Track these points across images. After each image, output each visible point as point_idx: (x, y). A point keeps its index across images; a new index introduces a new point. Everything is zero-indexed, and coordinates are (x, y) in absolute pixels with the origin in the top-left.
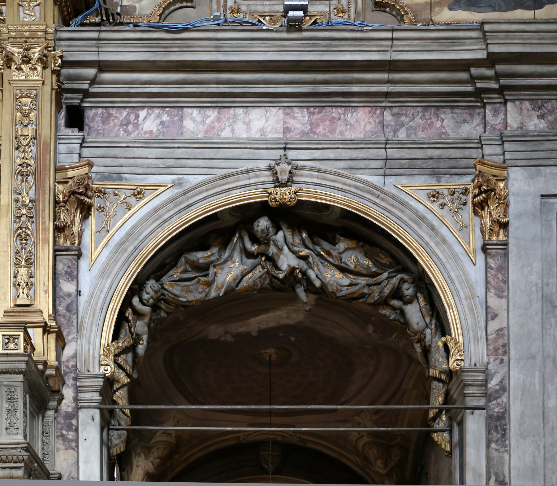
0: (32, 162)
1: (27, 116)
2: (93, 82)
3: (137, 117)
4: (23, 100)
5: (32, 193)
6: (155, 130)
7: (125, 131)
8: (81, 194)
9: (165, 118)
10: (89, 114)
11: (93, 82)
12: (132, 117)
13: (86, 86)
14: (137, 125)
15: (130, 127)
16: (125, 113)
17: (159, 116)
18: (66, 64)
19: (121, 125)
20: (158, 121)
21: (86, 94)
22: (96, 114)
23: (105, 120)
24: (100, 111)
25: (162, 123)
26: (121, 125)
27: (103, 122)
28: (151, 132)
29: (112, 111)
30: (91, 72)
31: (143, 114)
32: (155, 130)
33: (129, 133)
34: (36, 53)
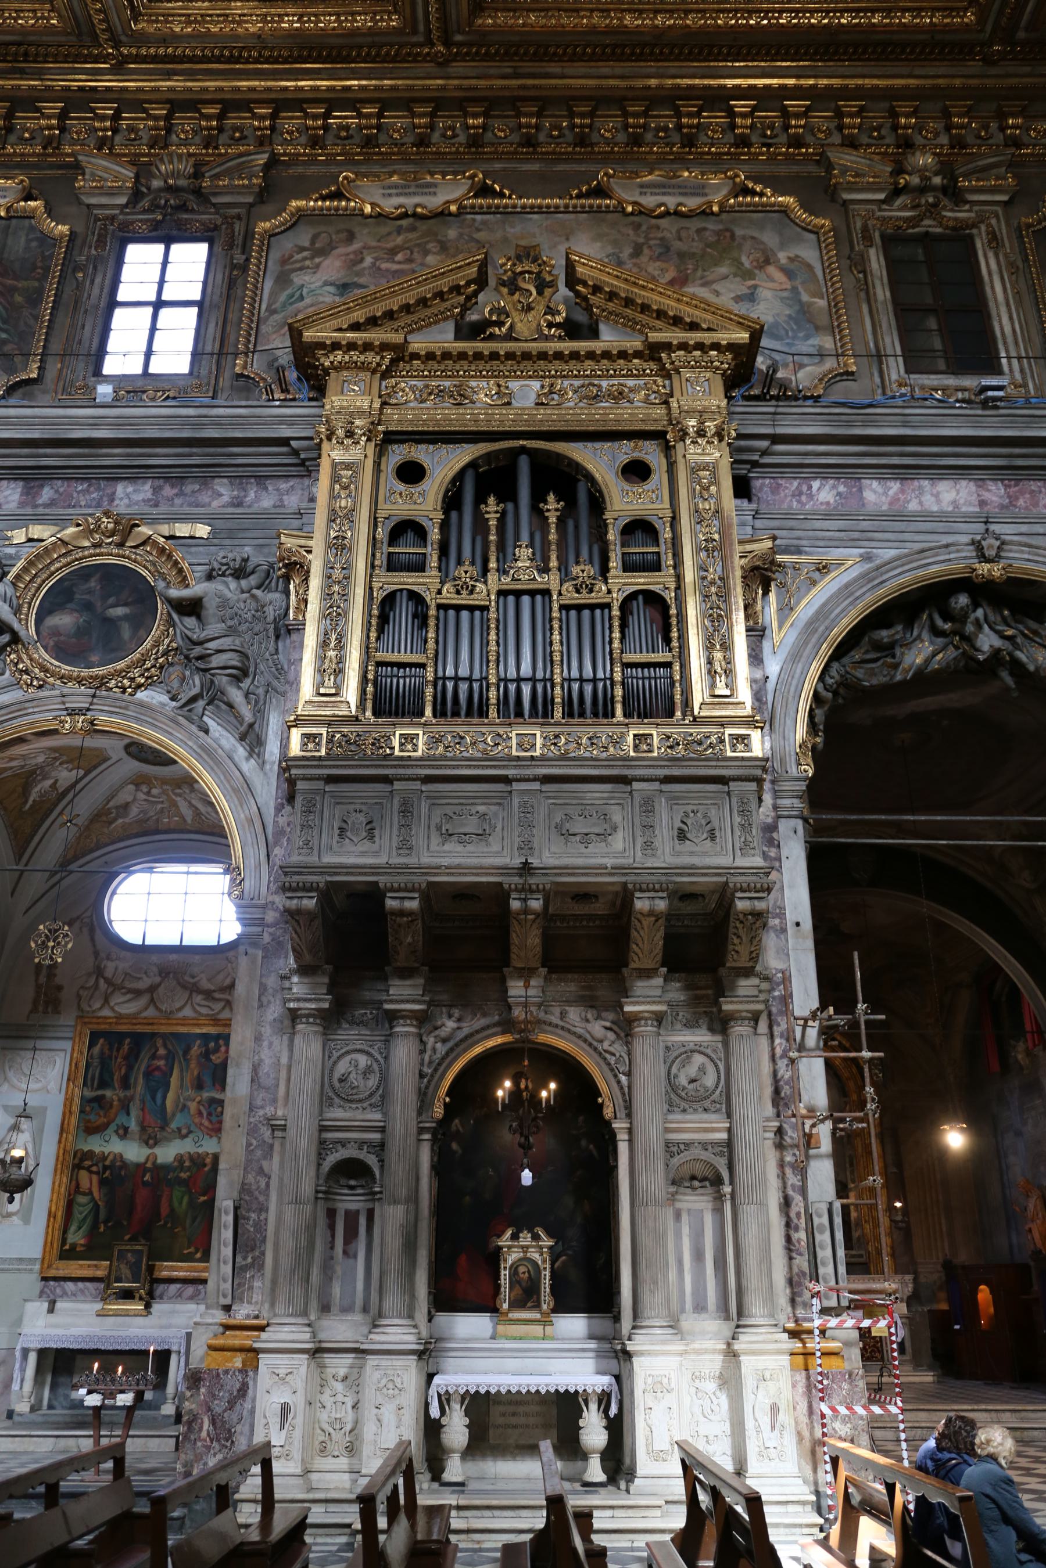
0: (716, 537)
1: (707, 489)
2: (764, 453)
3: (810, 487)
4: (701, 473)
5: (719, 569)
6: (832, 501)
7: (799, 502)
8: (766, 570)
9: (842, 488)
10: (756, 484)
11: (764, 453)
12: (805, 488)
13: (756, 458)
14: (811, 496)
15: (804, 498)
16: (796, 483)
17: (834, 487)
18: (740, 436)
19: (793, 496)
20: (834, 492)
21: (755, 464)
22: (763, 485)
23: (775, 490)
24: (767, 481)
25: (839, 494)
26: (793, 496)
27: (773, 493)
28: (828, 503)
29: (780, 481)
30: (764, 444)
31: (816, 484)
32: (832, 501)
33: (804, 505)
34: (711, 426)
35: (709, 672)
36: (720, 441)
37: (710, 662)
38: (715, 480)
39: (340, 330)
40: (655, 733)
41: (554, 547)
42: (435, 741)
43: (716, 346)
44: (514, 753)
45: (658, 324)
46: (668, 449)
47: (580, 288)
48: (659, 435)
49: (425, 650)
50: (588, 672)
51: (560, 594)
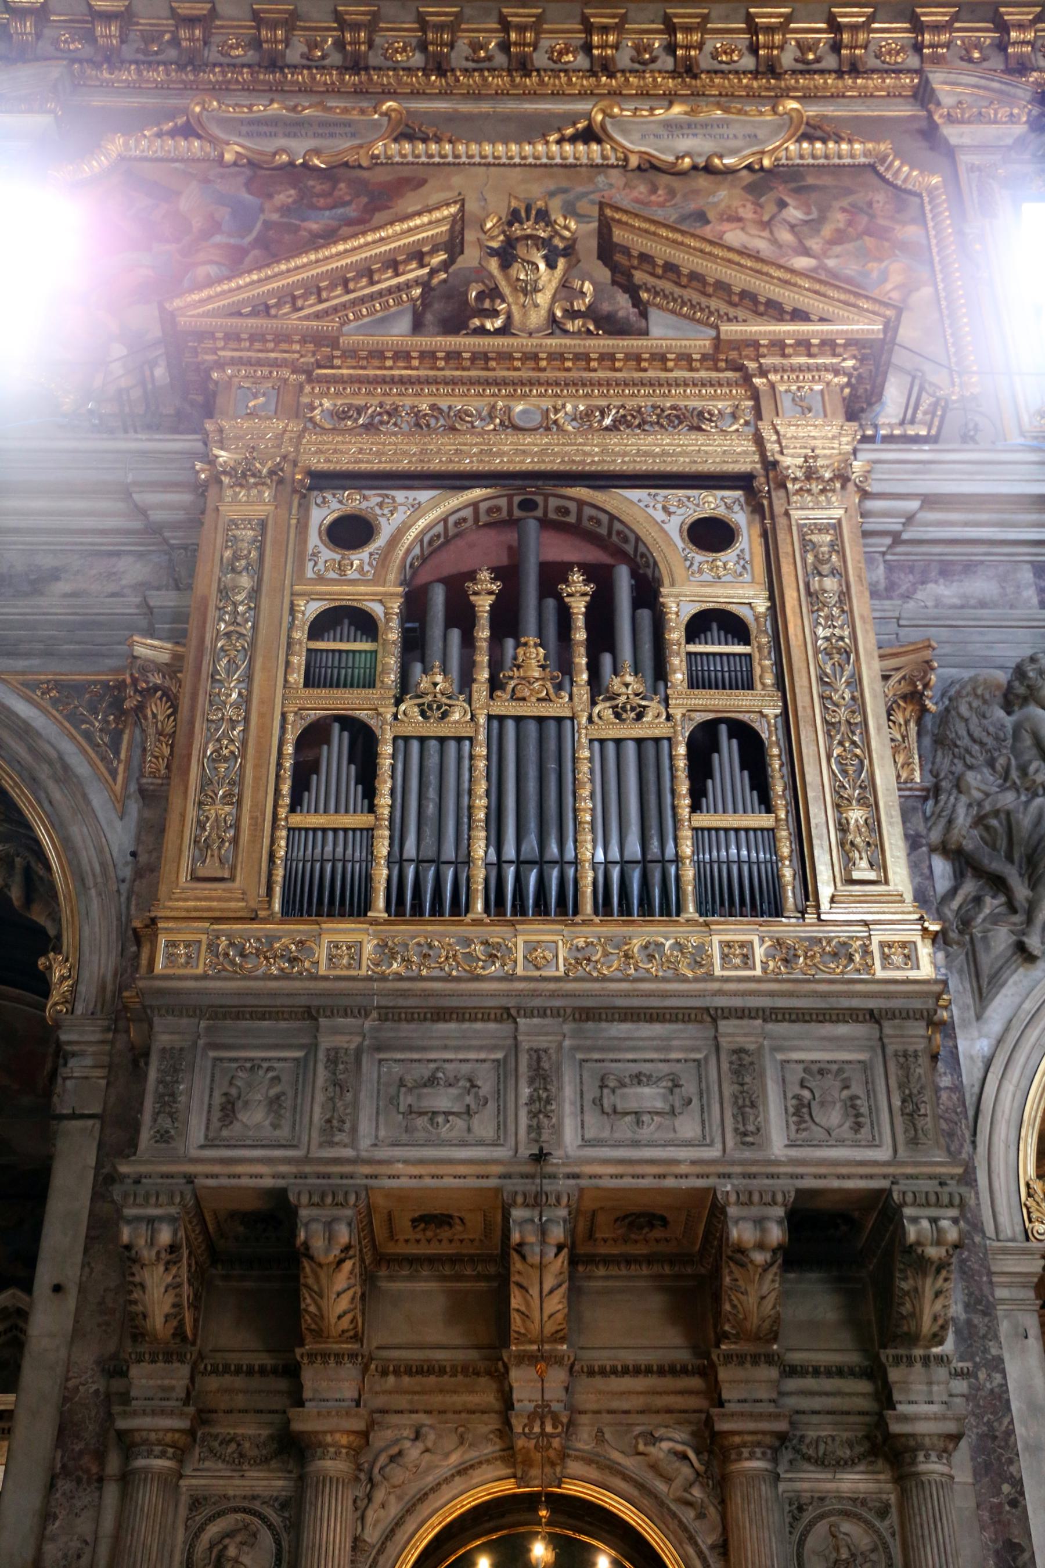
35: (842, 844)
36: (843, 487)
37: (843, 828)
38: (837, 546)
39: (240, 314)
40: (756, 940)
41: (582, 650)
42: (387, 951)
43: (829, 345)
44: (520, 971)
45: (741, 313)
46: (757, 507)
47: (618, 257)
48: (743, 481)
49: (372, 809)
50: (634, 849)
51: (590, 720)
